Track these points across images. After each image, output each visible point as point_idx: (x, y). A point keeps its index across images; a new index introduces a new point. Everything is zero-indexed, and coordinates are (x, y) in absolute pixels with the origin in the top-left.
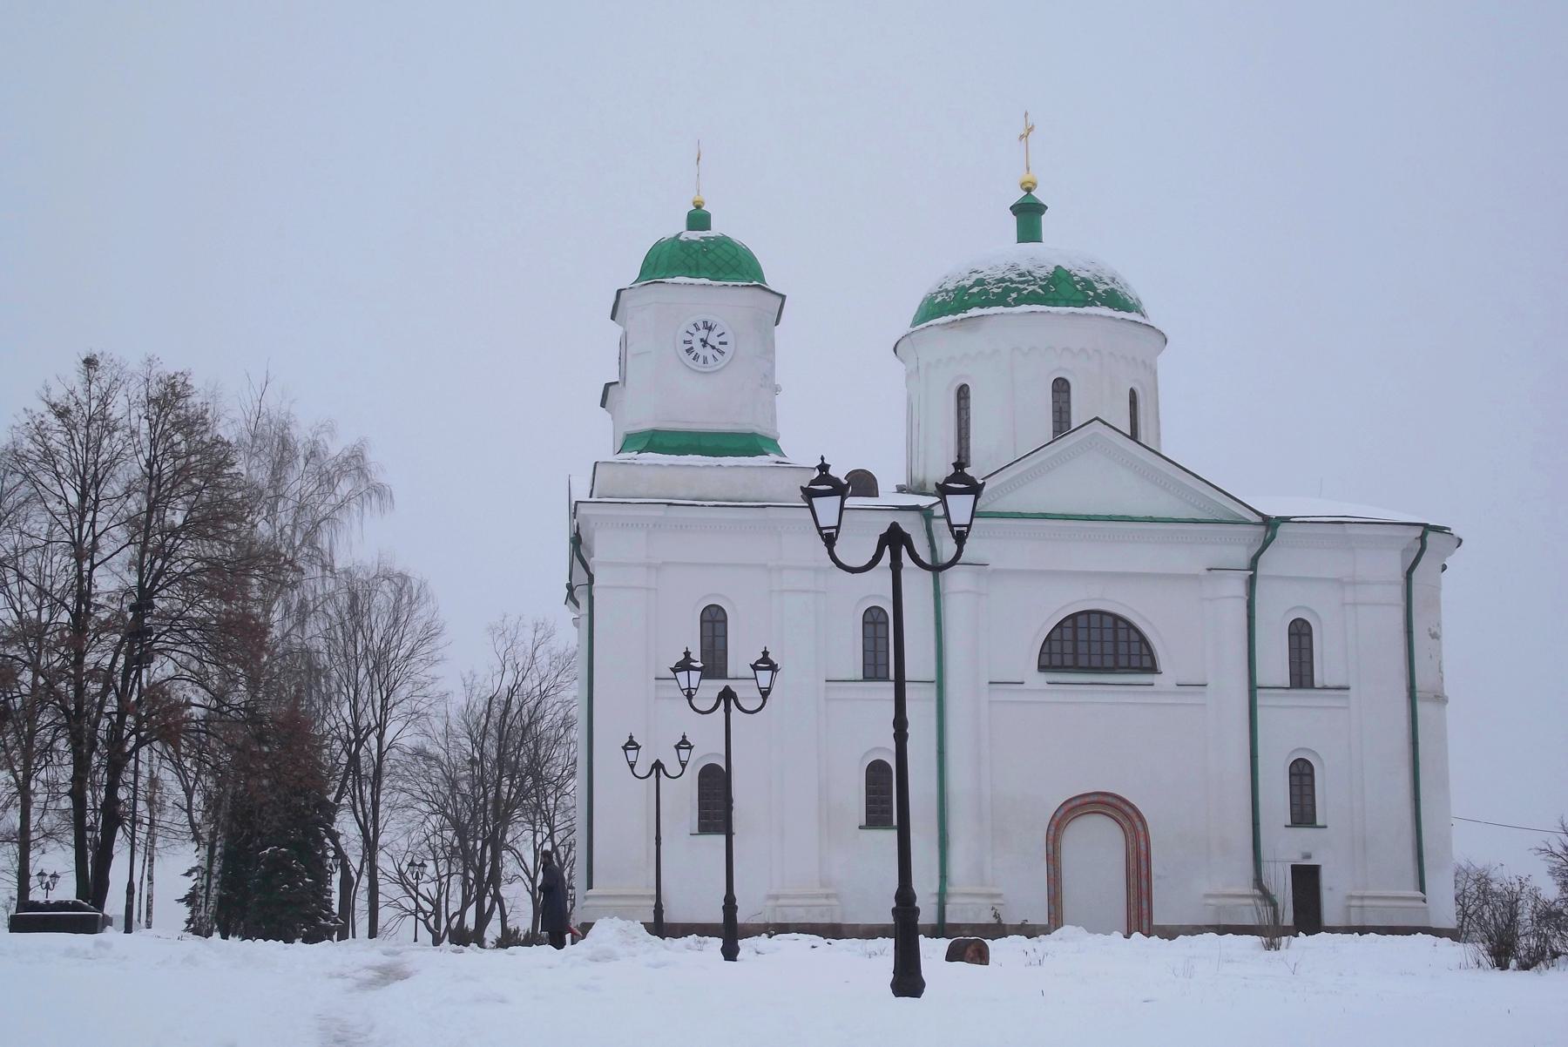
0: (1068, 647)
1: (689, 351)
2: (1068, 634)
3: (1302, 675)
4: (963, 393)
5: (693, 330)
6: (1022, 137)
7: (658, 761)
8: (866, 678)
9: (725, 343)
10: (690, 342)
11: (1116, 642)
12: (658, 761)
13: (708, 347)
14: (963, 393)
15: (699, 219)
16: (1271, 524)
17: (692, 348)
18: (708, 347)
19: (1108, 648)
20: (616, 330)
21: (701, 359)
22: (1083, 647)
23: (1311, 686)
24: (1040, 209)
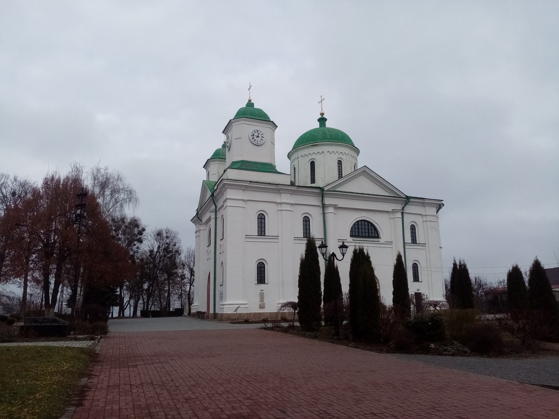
0: (357, 230)
1: (253, 138)
2: (356, 226)
3: (414, 241)
4: (313, 164)
6: (319, 102)
7: (333, 253)
9: (263, 137)
11: (368, 229)
12: (333, 253)
14: (313, 164)
15: (250, 104)
16: (408, 198)
17: (254, 138)
19: (367, 231)
20: (223, 138)
21: (256, 141)
22: (360, 230)
23: (416, 243)
24: (325, 120)
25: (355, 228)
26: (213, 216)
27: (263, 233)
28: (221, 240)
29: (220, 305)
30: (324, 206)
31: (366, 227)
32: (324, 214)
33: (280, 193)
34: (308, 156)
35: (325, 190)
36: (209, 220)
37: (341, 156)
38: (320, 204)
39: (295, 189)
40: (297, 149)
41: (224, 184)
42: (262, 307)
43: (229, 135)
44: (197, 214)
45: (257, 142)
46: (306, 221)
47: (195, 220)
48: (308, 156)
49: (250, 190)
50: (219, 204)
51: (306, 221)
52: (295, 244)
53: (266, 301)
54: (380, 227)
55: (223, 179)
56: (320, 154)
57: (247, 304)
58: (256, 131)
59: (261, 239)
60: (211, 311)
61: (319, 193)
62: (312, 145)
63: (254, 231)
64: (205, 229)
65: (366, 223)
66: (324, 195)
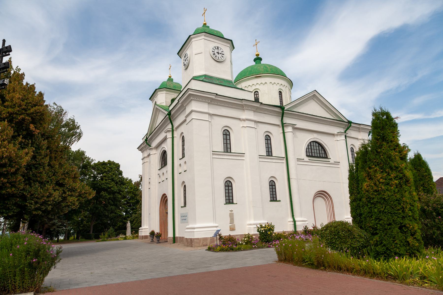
1: (214, 54)
2: (310, 146)
5: (214, 49)
6: (254, 46)
8: (267, 156)
9: (224, 54)
10: (214, 52)
13: (220, 54)
16: (350, 122)
17: (215, 54)
18: (220, 54)
24: (261, 59)
25: (309, 149)
26: (169, 135)
27: (229, 150)
28: (180, 159)
29: (186, 228)
30: (283, 125)
32: (284, 133)
33: (244, 110)
34: (251, 86)
36: (165, 139)
37: (281, 87)
38: (279, 123)
39: (259, 106)
40: (240, 80)
41: (190, 94)
42: (232, 229)
43: (188, 53)
44: (146, 140)
45: (218, 58)
46: (268, 139)
47: (143, 147)
48: (251, 86)
49: (215, 104)
50: (176, 123)
51: (268, 139)
52: (260, 162)
53: (236, 222)
54: (329, 148)
55: (188, 89)
56: (264, 84)
57: (218, 226)
58: (217, 48)
59: (227, 156)
60: (170, 235)
61: (279, 112)
62: (256, 77)
63: (220, 147)
64: (155, 154)
66: (284, 115)
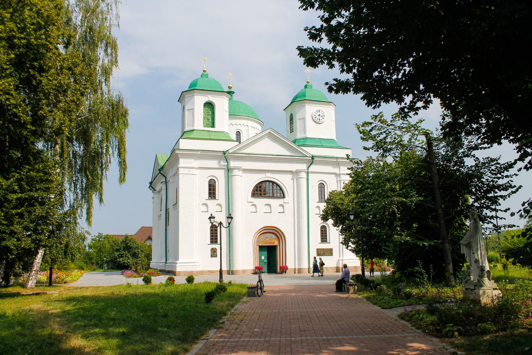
30: (229, 170)
31: (271, 188)
35: (230, 152)
65: (271, 184)
